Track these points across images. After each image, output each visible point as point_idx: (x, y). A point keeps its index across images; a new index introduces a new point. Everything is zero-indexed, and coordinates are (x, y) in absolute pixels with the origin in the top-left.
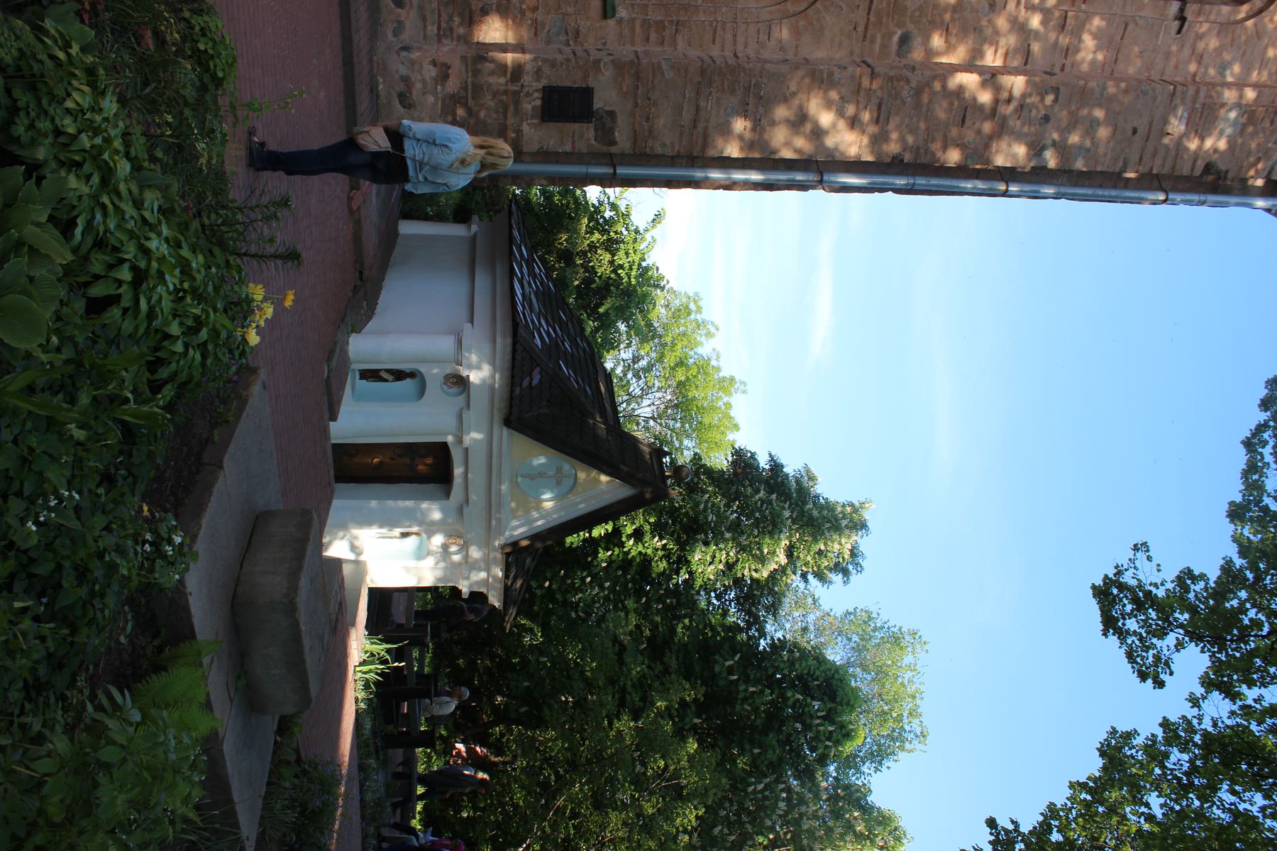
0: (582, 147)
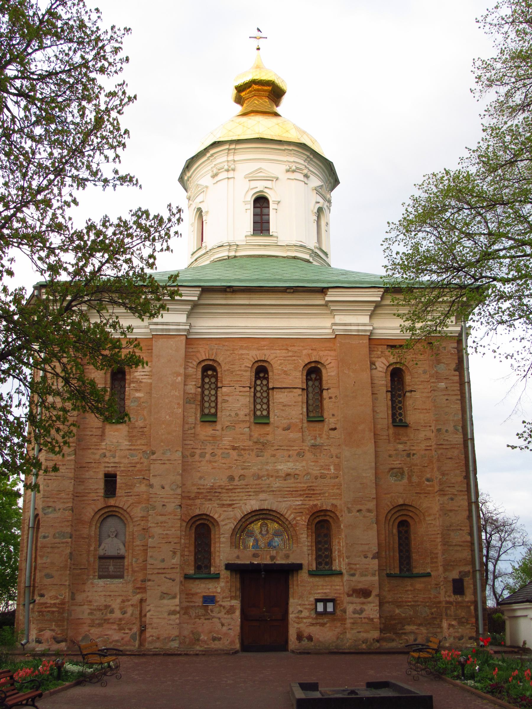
0: (471, 581)
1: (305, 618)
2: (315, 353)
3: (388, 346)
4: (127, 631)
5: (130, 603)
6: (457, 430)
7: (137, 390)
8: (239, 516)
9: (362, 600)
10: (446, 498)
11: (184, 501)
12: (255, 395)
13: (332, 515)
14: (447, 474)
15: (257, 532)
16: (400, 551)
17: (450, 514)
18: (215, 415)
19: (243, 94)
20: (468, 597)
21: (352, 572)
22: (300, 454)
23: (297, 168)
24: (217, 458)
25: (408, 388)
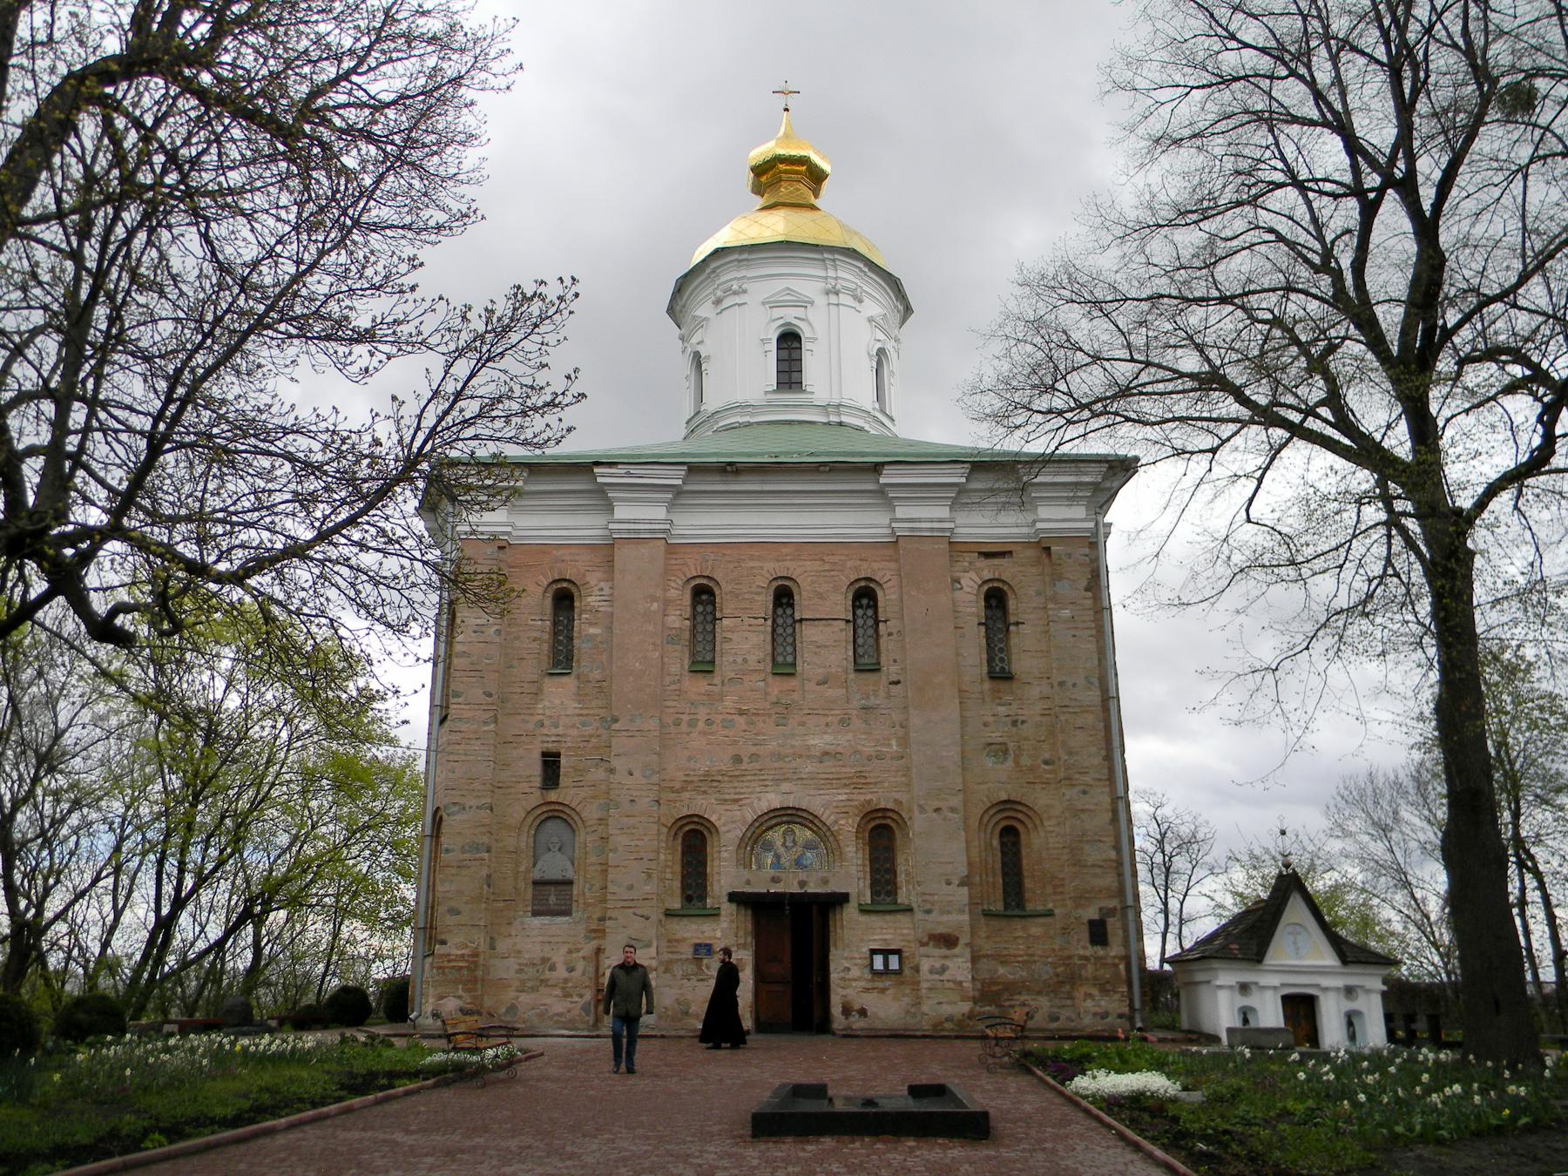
0: (1119, 924)
1: (855, 980)
2: (865, 565)
3: (980, 553)
4: (576, 999)
5: (581, 954)
6: (1091, 683)
7: (591, 624)
8: (750, 817)
9: (944, 951)
10: (1077, 789)
11: (665, 796)
12: (774, 630)
13: (895, 816)
14: (1077, 753)
15: (779, 843)
16: (1005, 874)
17: (1083, 816)
18: (712, 662)
19: (763, 179)
20: (1115, 950)
21: (928, 906)
22: (844, 722)
23: (843, 287)
24: (714, 727)
25: (1012, 619)
